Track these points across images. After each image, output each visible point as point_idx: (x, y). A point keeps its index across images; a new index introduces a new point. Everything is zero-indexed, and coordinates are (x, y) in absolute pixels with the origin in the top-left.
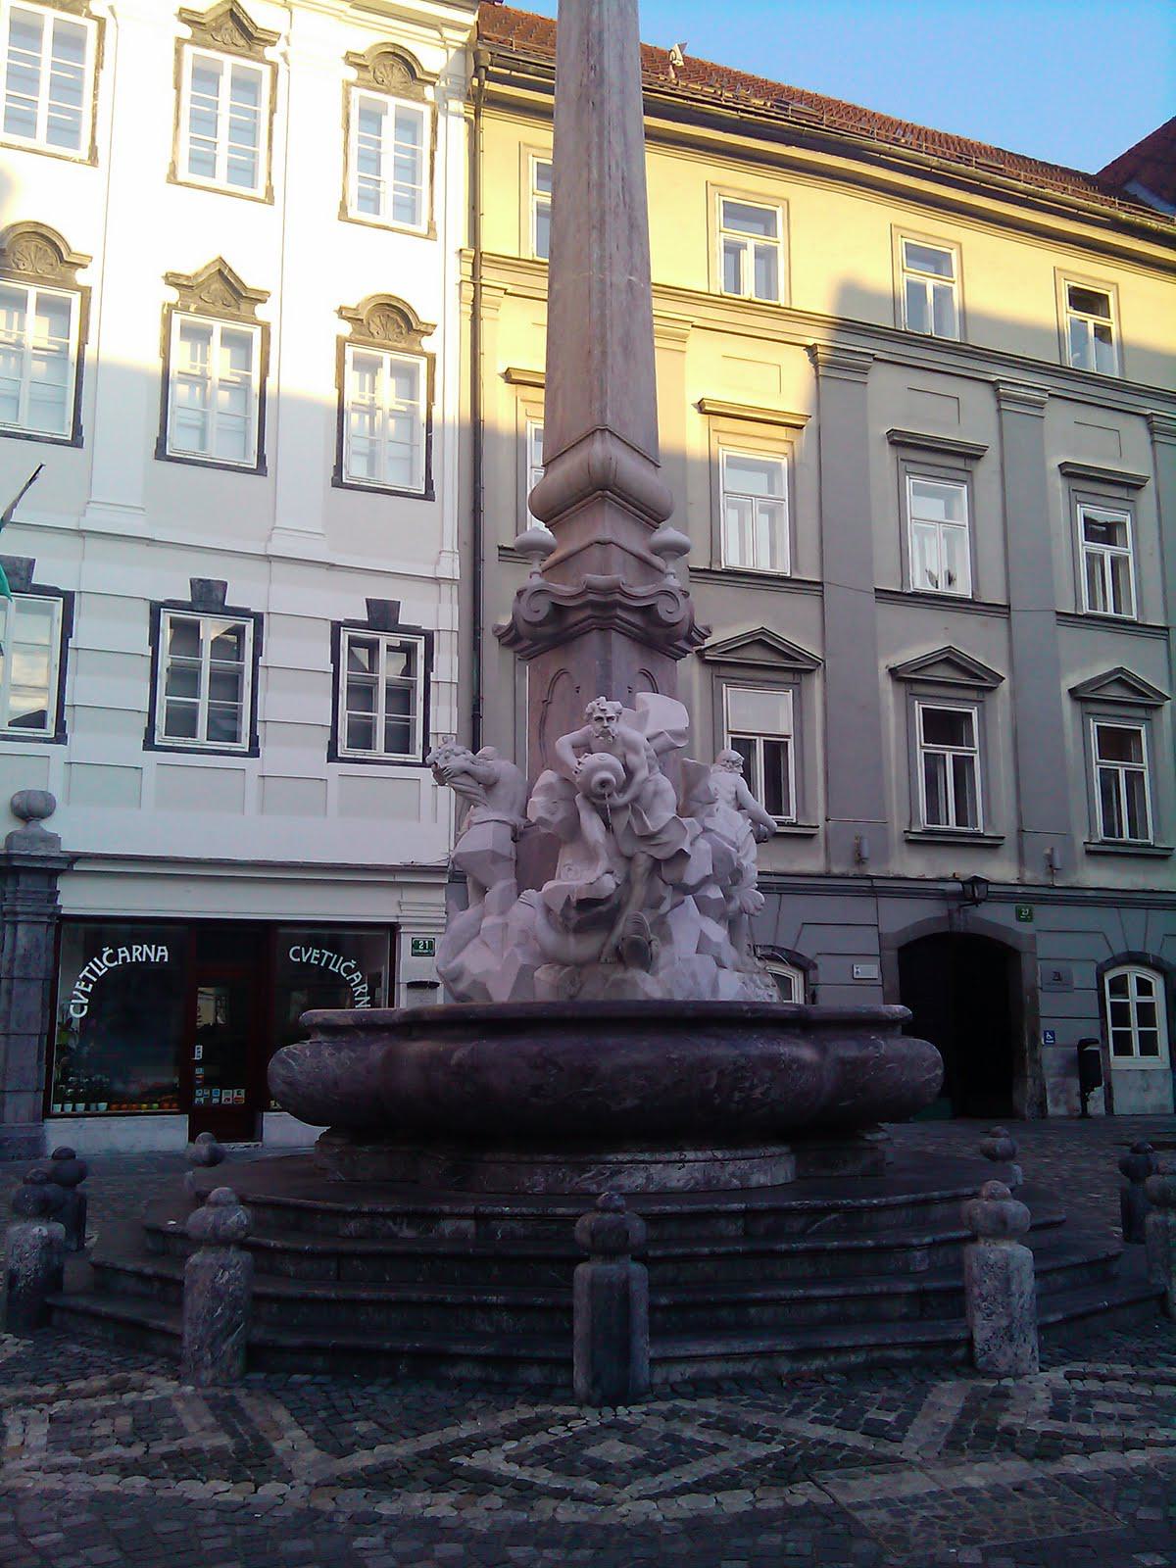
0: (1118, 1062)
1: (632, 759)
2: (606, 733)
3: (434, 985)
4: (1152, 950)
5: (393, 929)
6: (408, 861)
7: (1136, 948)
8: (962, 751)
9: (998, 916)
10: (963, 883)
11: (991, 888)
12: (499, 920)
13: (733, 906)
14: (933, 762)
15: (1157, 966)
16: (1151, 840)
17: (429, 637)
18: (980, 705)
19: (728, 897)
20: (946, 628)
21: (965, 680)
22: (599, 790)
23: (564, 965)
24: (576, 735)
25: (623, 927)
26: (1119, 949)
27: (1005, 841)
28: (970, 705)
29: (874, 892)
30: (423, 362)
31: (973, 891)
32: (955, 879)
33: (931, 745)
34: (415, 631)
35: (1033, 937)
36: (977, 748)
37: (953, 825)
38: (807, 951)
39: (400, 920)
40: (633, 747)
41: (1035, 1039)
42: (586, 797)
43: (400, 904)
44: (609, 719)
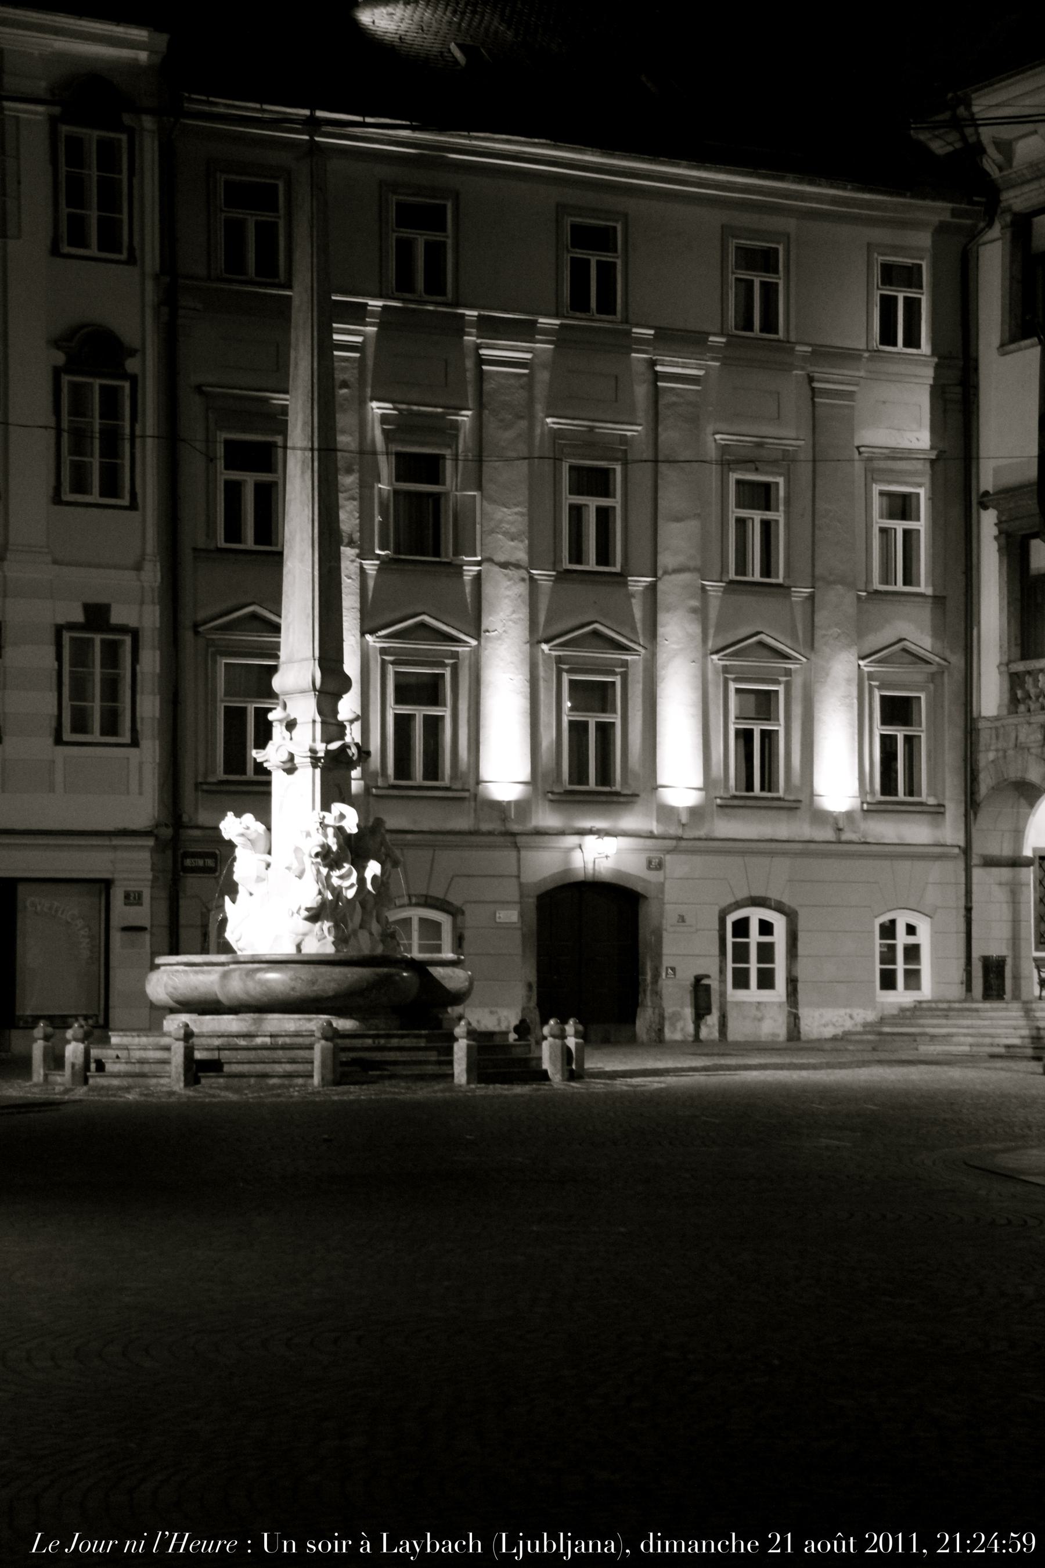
0: (735, 995)
3: (141, 929)
4: (774, 895)
5: (107, 884)
6: (121, 826)
7: (755, 893)
15: (780, 908)
16: (781, 793)
17: (135, 634)
26: (742, 894)
30: (127, 385)
34: (123, 629)
35: (663, 884)
38: (455, 899)
39: (116, 876)
41: (656, 976)
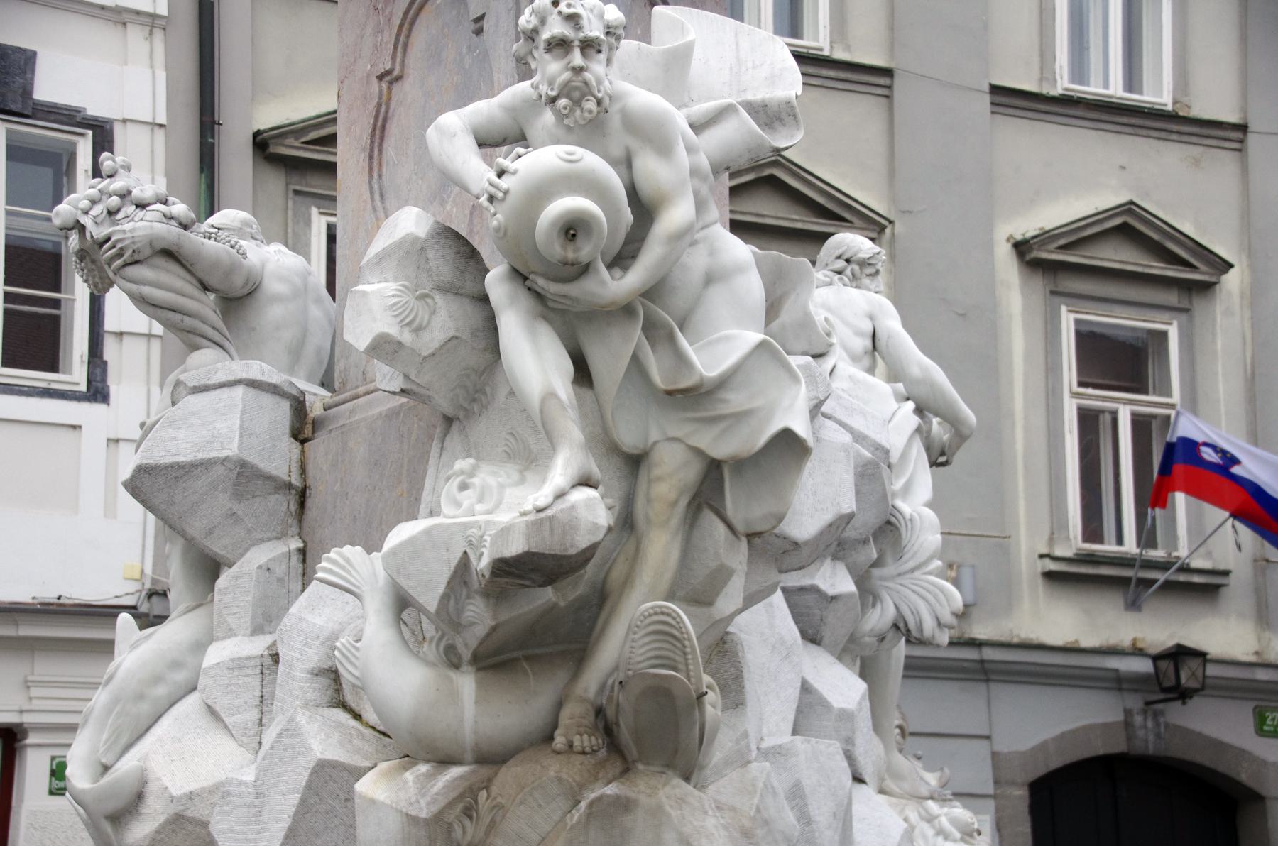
1: (651, 169)
2: (575, 92)
6: (48, 593)
8: (1149, 403)
9: (1219, 727)
10: (1156, 658)
11: (1211, 670)
12: (257, 646)
13: (879, 618)
14: (1088, 419)
18: (1184, 317)
19: (867, 593)
20: (1123, 168)
21: (1158, 268)
22: (557, 250)
23: (445, 761)
24: (484, 109)
25: (619, 646)
27: (1232, 580)
28: (1166, 316)
29: (985, 673)
31: (1176, 675)
32: (1137, 651)
33: (1090, 391)
36: (1176, 398)
37: (1130, 546)
39: (27, 719)
40: (652, 134)
42: (519, 275)
43: (27, 685)
44: (589, 46)
